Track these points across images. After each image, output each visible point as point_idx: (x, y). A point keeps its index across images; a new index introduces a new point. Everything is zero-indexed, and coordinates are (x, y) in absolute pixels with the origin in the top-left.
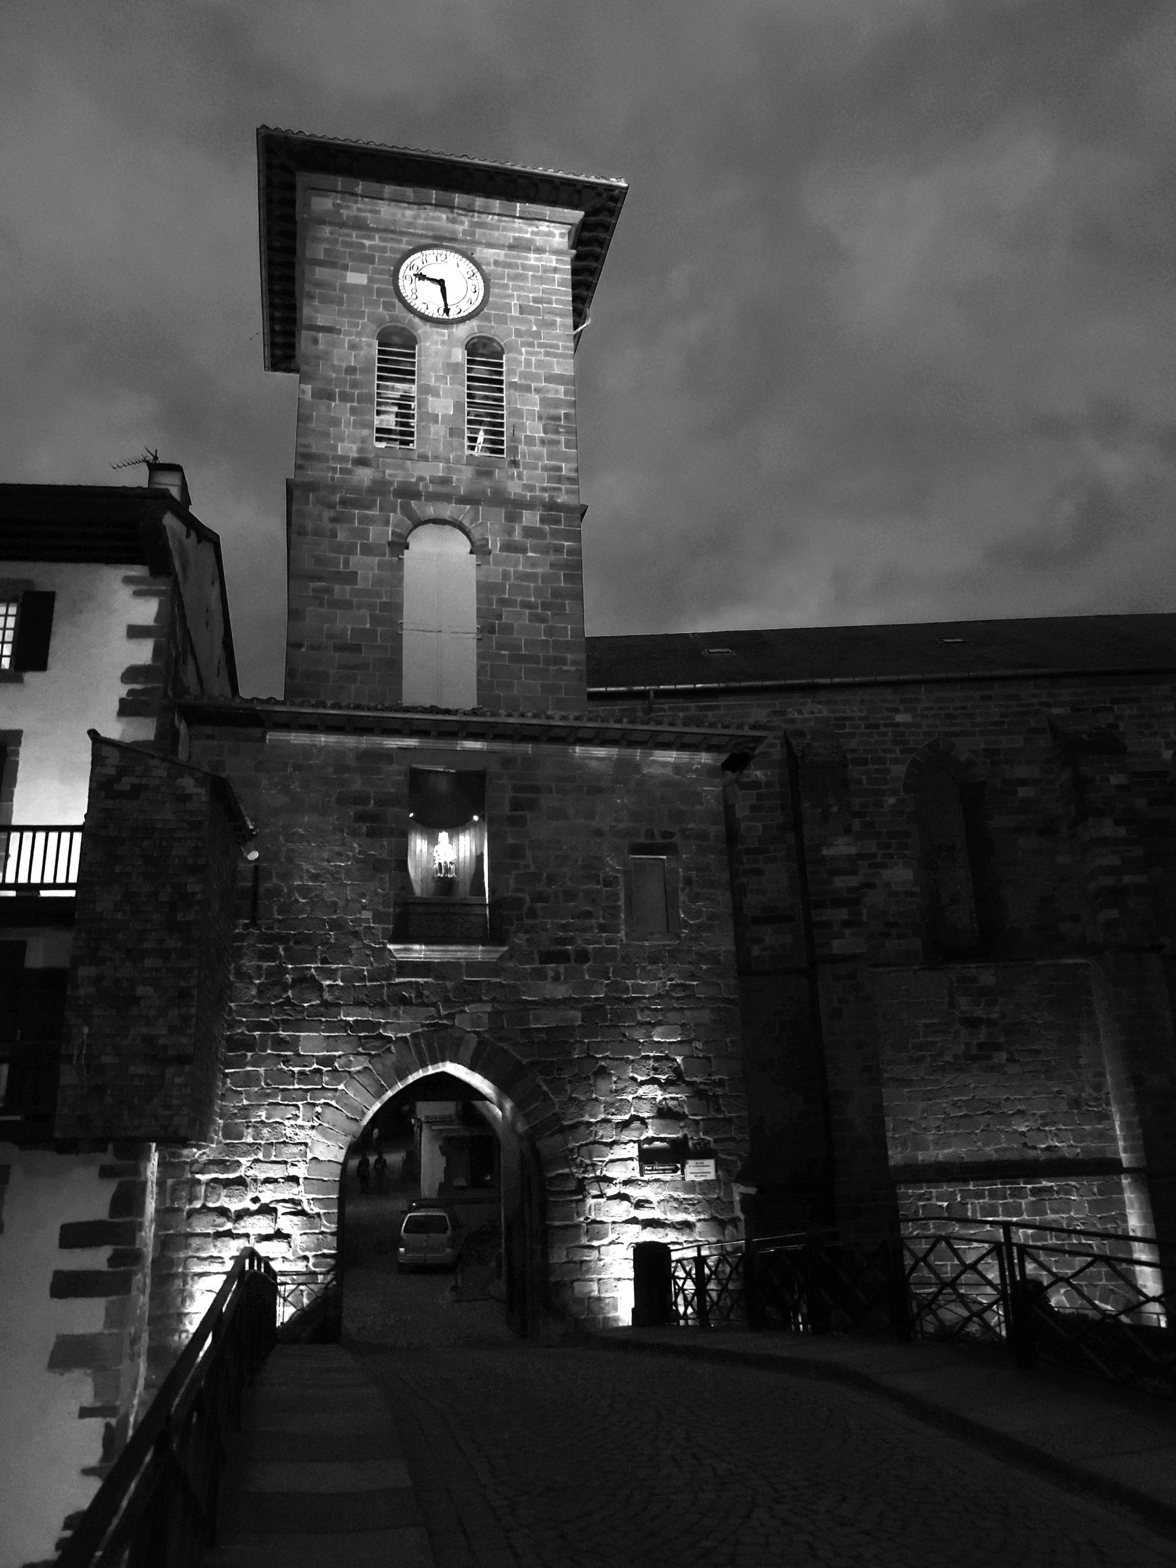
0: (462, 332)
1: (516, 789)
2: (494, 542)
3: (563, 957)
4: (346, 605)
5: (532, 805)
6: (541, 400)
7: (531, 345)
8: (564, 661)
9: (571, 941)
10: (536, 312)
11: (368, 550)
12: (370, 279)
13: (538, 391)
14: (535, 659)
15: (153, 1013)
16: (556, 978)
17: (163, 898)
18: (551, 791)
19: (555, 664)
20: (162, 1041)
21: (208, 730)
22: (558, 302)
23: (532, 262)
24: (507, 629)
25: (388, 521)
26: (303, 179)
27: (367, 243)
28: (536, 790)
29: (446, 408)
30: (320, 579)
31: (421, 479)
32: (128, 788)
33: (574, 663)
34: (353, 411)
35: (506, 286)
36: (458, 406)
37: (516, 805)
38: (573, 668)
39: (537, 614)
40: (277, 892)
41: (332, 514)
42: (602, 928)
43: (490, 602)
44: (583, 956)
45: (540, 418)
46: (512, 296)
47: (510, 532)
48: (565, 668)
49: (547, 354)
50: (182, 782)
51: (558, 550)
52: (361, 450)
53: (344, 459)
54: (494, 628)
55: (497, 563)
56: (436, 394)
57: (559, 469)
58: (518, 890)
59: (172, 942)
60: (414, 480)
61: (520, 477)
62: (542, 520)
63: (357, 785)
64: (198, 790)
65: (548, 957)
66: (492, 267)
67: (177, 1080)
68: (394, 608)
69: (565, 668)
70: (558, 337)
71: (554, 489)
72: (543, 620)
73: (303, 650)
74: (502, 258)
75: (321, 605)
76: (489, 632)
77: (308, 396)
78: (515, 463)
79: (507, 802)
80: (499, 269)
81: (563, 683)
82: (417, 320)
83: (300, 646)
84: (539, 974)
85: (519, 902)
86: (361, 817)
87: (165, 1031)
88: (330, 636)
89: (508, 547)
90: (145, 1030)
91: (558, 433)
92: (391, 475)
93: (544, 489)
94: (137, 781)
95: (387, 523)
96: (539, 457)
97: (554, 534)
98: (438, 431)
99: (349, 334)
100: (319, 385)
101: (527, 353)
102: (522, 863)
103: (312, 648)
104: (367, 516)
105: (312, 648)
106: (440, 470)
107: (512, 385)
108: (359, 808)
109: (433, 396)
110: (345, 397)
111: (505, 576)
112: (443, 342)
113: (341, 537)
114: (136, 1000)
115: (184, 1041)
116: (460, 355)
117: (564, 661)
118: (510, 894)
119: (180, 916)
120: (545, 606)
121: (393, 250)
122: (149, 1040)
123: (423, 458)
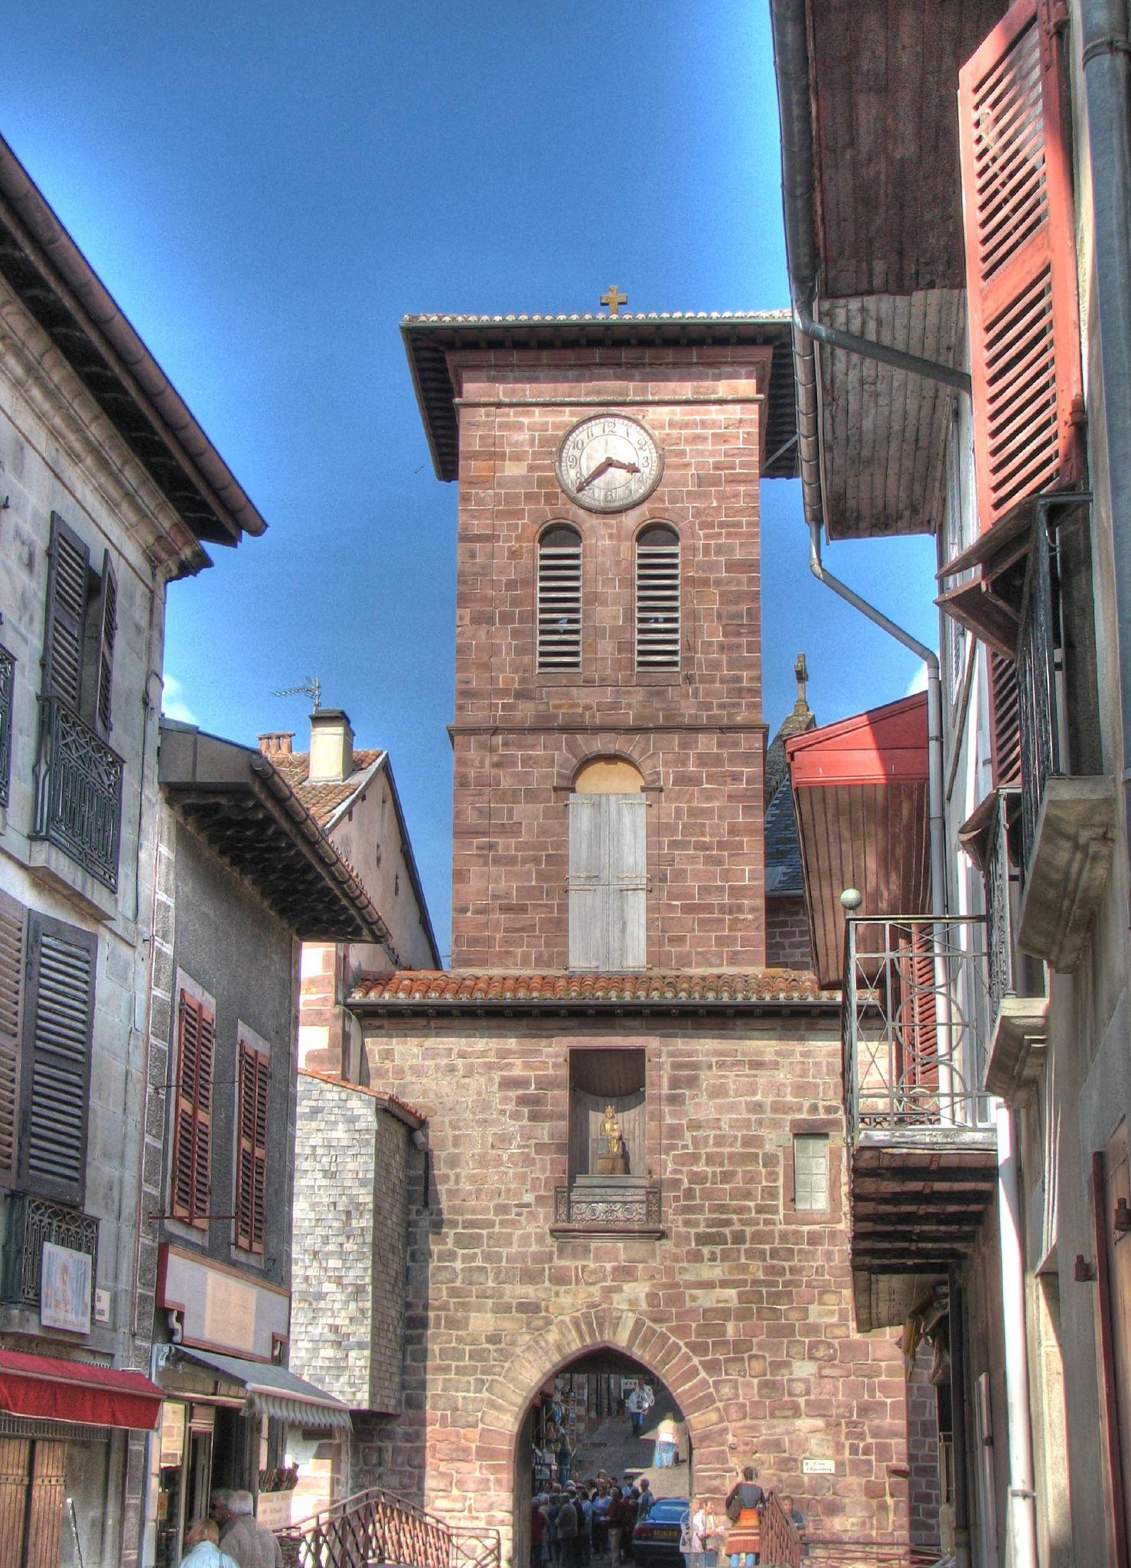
0: (632, 521)
1: (676, 1066)
2: (667, 774)
3: (720, 1239)
4: (510, 861)
5: (692, 1082)
6: (722, 595)
7: (711, 525)
8: (740, 909)
9: (728, 1223)
10: (716, 482)
11: (532, 796)
12: (531, 468)
13: (718, 583)
14: (708, 908)
15: (337, 1306)
16: (713, 1259)
17: (340, 1208)
18: (710, 1067)
19: (731, 912)
20: (344, 1330)
21: (377, 1022)
22: (743, 465)
23: (714, 416)
24: (680, 875)
25: (553, 761)
26: (452, 359)
27: (526, 420)
28: (695, 1066)
29: (615, 618)
30: (484, 834)
31: (587, 708)
32: (307, 1110)
33: (753, 910)
34: (515, 634)
35: (683, 453)
36: (628, 616)
37: (675, 1083)
38: (750, 917)
39: (711, 856)
40: (446, 1178)
41: (495, 759)
42: (760, 1210)
43: (660, 845)
44: (739, 1238)
45: (719, 617)
46: (687, 465)
47: (684, 763)
48: (742, 917)
49: (729, 535)
50: (350, 1104)
51: (736, 777)
52: (523, 681)
53: (504, 692)
54: (665, 875)
55: (669, 800)
56: (604, 603)
57: (739, 679)
58: (675, 1171)
59: (349, 1246)
60: (580, 710)
61: (696, 695)
62: (720, 745)
63: (517, 1072)
64: (364, 1111)
65: (703, 1239)
66: (667, 431)
67: (359, 1363)
68: (559, 861)
69: (742, 917)
70: (740, 511)
71: (734, 705)
72: (719, 862)
73: (469, 914)
74: (678, 417)
75: (486, 864)
76: (661, 880)
77: (467, 621)
78: (689, 679)
79: (665, 1081)
80: (674, 431)
81: (739, 934)
82: (582, 512)
83: (465, 910)
84: (696, 1257)
85: (676, 1183)
86: (522, 1101)
87: (347, 1321)
88: (495, 897)
89: (683, 780)
90: (331, 1321)
91: (739, 634)
92: (556, 707)
93: (722, 706)
94: (313, 1103)
95: (552, 764)
96: (715, 665)
97: (732, 759)
98: (606, 648)
99: (508, 539)
100: (477, 607)
101: (707, 537)
102: (681, 1143)
103: (477, 912)
104: (530, 758)
105: (477, 912)
106: (608, 695)
107: (690, 581)
108: (520, 1092)
109: (601, 604)
110: (506, 618)
111: (678, 811)
112: (611, 536)
113: (506, 783)
114: (321, 1296)
115: (362, 1330)
116: (631, 550)
117: (740, 909)
118: (668, 1175)
119: (354, 1223)
120: (721, 845)
121: (556, 426)
122: (335, 1329)
123: (589, 683)
